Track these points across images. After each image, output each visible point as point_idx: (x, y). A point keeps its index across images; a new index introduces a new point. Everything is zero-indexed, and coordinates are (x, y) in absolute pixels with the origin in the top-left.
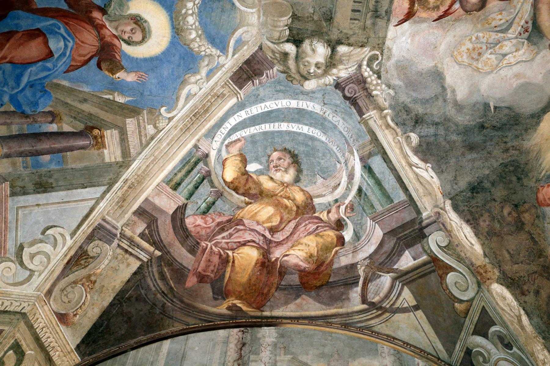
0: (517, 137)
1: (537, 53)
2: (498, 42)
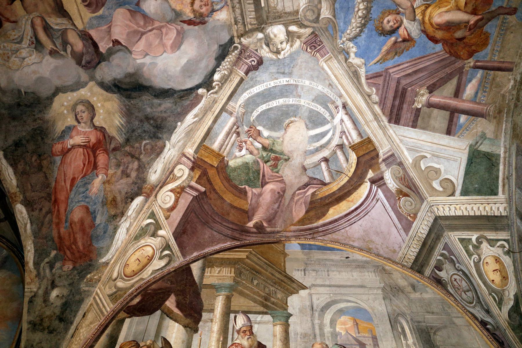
0: (40, 111)
1: (43, 58)
2: (17, 50)
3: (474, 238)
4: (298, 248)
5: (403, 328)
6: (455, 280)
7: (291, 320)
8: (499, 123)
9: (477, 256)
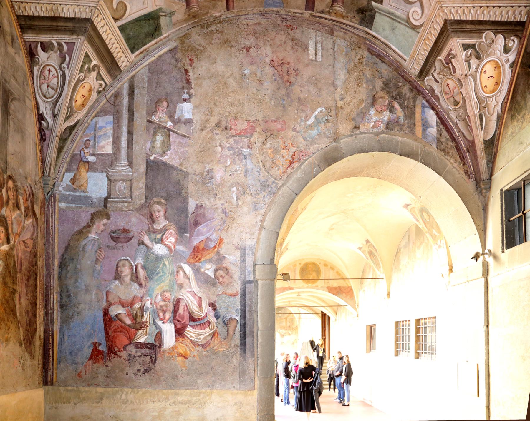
3: (94, 63)
6: (50, 71)
8: (186, 21)
9: (84, 76)
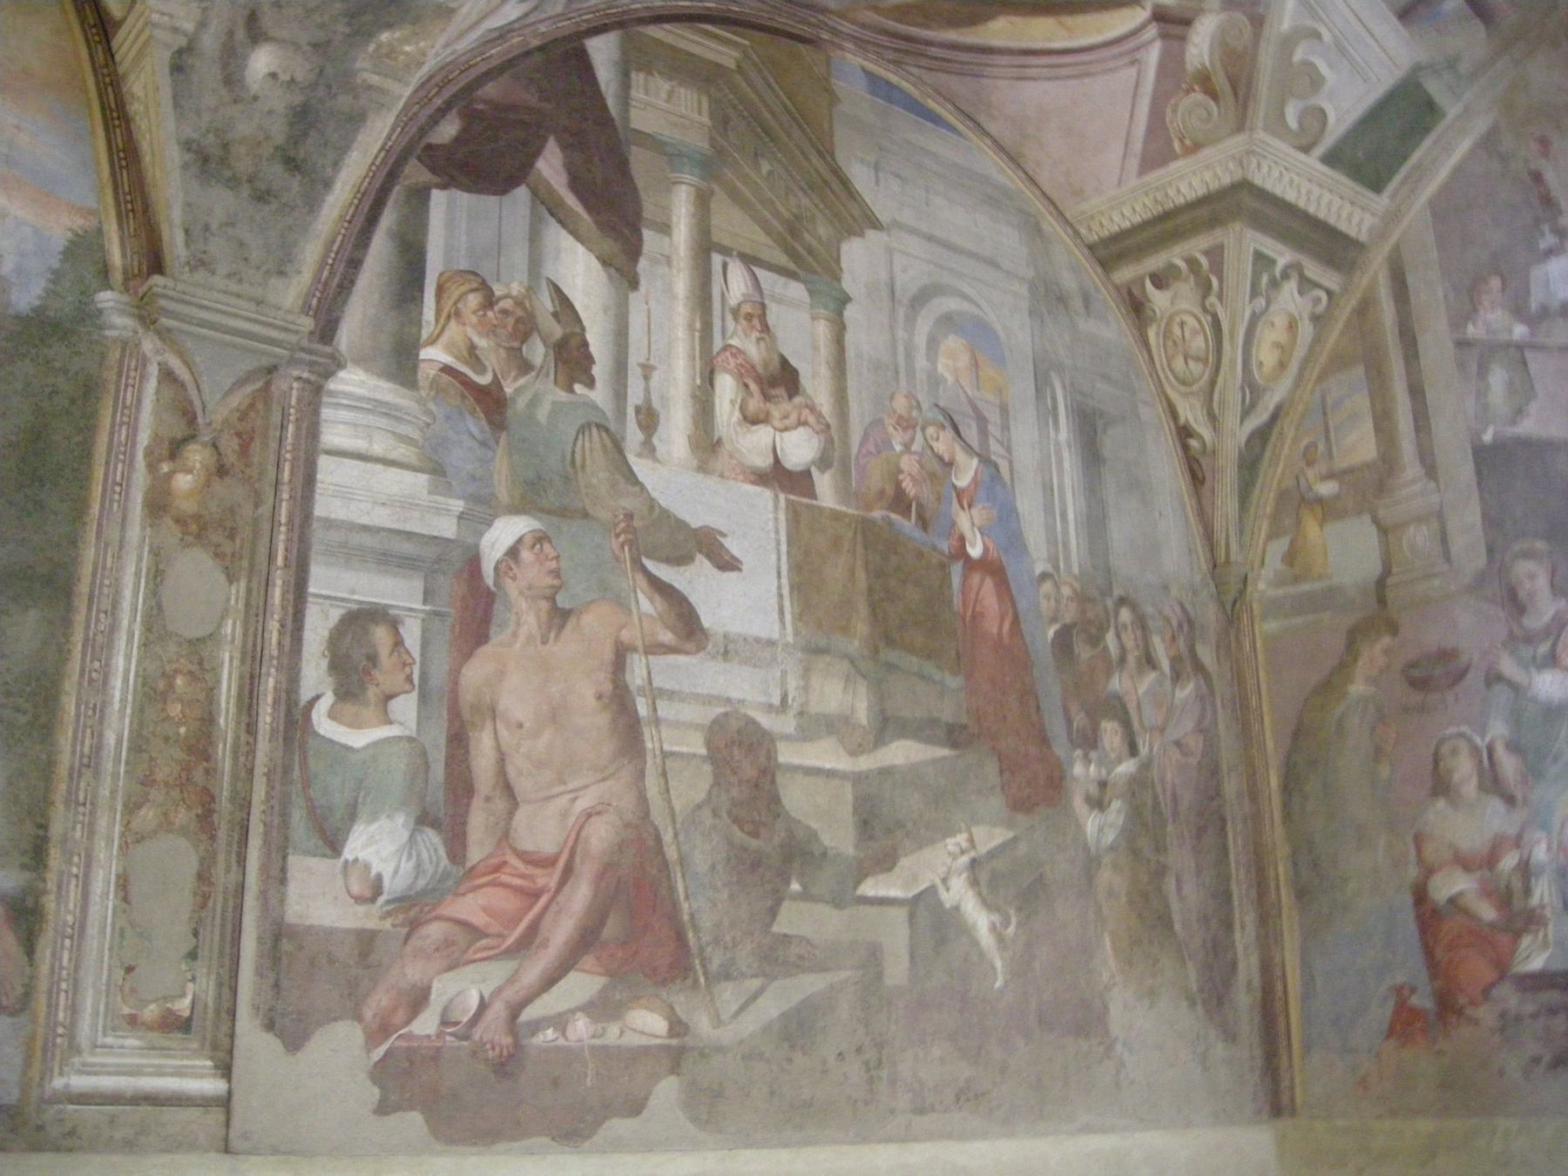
3: (1281, 262)
4: (860, 86)
5: (1054, 399)
6: (1182, 324)
7: (850, 312)
